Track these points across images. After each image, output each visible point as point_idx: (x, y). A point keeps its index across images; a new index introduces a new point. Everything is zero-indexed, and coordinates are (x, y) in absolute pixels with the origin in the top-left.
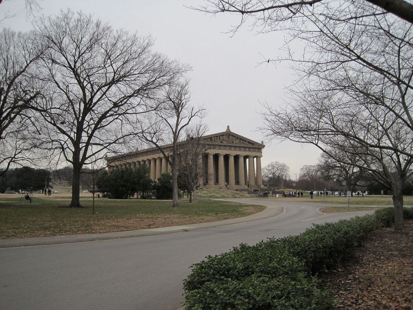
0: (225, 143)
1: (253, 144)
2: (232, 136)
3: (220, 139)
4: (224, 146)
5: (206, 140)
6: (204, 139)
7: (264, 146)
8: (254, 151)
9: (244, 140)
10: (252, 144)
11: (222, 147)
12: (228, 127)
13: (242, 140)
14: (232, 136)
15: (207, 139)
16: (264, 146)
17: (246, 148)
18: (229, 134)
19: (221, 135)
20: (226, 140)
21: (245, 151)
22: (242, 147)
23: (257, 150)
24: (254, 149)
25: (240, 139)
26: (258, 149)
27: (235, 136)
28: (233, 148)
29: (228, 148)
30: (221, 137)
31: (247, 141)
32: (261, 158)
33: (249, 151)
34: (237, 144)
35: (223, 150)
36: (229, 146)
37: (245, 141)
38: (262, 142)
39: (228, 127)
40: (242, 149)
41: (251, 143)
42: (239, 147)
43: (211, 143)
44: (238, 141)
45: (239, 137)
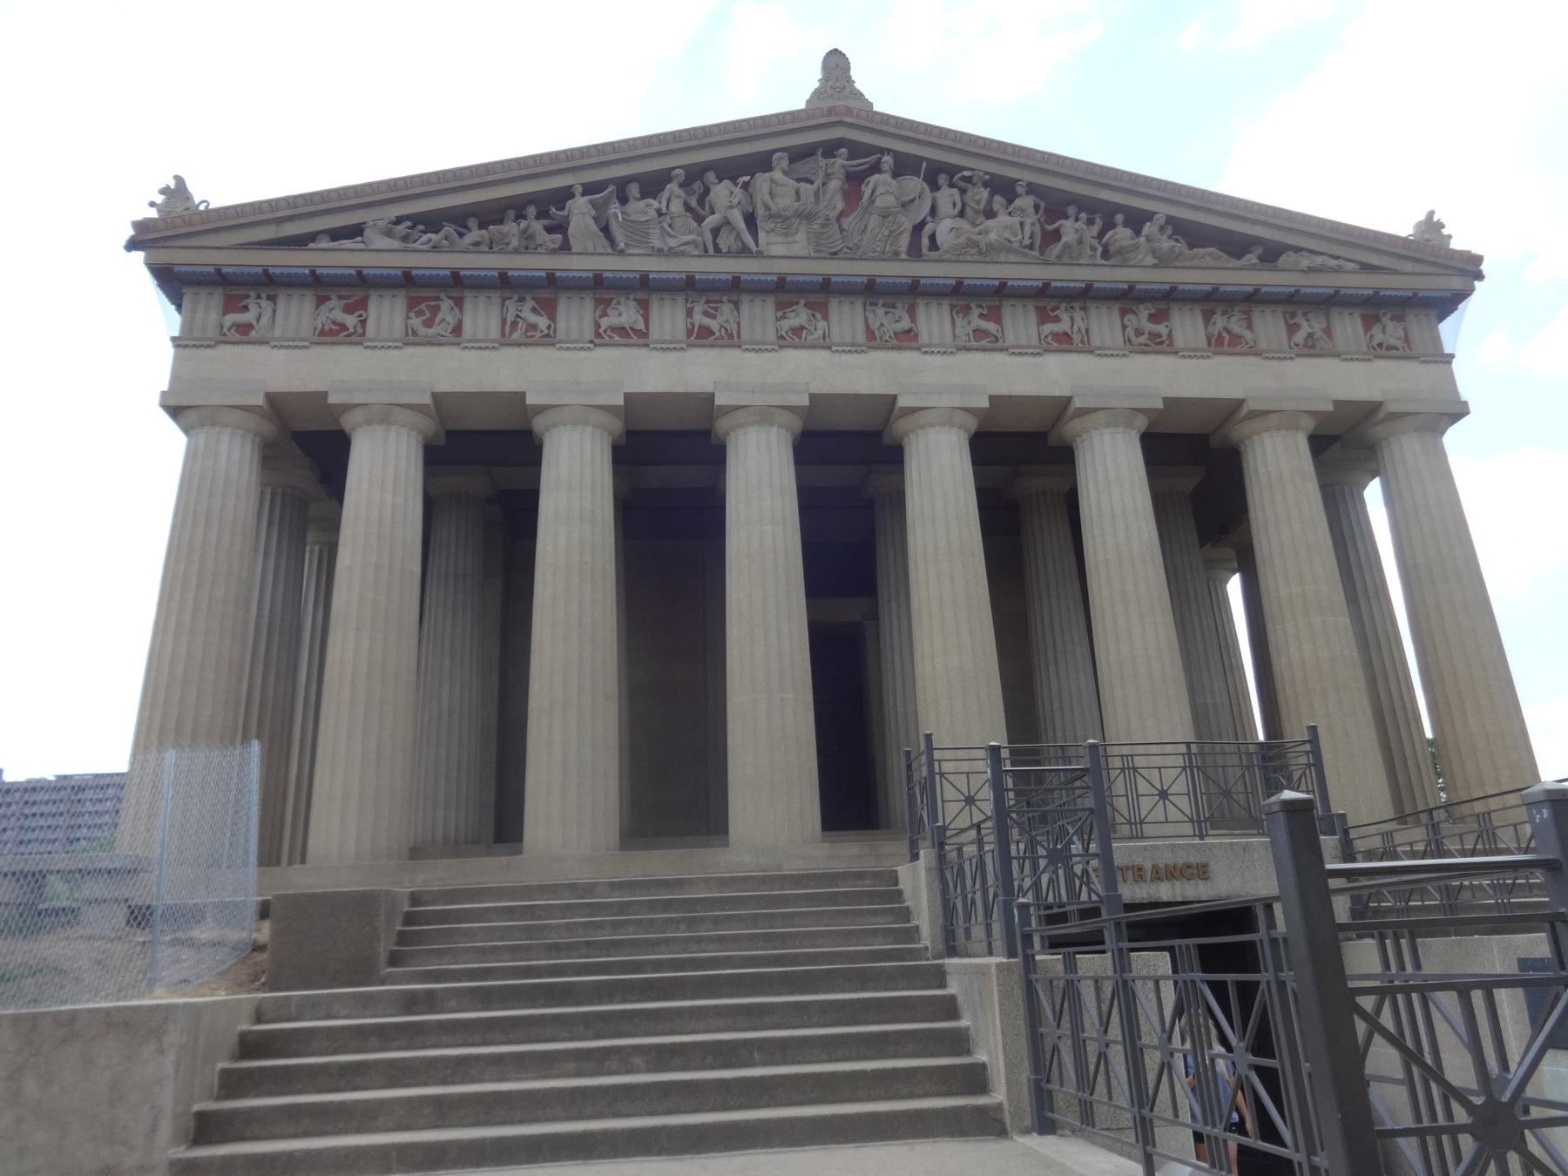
1: (1272, 254)
2: (904, 166)
3: (700, 220)
4: (782, 291)
5: (475, 235)
6: (431, 222)
7: (1469, 269)
10: (1251, 258)
11: (758, 316)
12: (836, 64)
14: (904, 166)
15: (490, 215)
16: (1469, 269)
18: (856, 150)
19: (730, 170)
20: (807, 217)
21: (1160, 345)
22: (1086, 295)
23: (1348, 328)
24: (1310, 325)
26: (1374, 307)
27: (952, 170)
29: (846, 319)
30: (722, 193)
31: (1163, 210)
32: (1454, 439)
33: (1222, 344)
34: (988, 253)
35: (758, 347)
36: (871, 291)
37: (1137, 220)
38: (1431, 226)
39: (836, 64)
40: (1104, 324)
41: (1236, 246)
42: (1046, 298)
43: (536, 263)
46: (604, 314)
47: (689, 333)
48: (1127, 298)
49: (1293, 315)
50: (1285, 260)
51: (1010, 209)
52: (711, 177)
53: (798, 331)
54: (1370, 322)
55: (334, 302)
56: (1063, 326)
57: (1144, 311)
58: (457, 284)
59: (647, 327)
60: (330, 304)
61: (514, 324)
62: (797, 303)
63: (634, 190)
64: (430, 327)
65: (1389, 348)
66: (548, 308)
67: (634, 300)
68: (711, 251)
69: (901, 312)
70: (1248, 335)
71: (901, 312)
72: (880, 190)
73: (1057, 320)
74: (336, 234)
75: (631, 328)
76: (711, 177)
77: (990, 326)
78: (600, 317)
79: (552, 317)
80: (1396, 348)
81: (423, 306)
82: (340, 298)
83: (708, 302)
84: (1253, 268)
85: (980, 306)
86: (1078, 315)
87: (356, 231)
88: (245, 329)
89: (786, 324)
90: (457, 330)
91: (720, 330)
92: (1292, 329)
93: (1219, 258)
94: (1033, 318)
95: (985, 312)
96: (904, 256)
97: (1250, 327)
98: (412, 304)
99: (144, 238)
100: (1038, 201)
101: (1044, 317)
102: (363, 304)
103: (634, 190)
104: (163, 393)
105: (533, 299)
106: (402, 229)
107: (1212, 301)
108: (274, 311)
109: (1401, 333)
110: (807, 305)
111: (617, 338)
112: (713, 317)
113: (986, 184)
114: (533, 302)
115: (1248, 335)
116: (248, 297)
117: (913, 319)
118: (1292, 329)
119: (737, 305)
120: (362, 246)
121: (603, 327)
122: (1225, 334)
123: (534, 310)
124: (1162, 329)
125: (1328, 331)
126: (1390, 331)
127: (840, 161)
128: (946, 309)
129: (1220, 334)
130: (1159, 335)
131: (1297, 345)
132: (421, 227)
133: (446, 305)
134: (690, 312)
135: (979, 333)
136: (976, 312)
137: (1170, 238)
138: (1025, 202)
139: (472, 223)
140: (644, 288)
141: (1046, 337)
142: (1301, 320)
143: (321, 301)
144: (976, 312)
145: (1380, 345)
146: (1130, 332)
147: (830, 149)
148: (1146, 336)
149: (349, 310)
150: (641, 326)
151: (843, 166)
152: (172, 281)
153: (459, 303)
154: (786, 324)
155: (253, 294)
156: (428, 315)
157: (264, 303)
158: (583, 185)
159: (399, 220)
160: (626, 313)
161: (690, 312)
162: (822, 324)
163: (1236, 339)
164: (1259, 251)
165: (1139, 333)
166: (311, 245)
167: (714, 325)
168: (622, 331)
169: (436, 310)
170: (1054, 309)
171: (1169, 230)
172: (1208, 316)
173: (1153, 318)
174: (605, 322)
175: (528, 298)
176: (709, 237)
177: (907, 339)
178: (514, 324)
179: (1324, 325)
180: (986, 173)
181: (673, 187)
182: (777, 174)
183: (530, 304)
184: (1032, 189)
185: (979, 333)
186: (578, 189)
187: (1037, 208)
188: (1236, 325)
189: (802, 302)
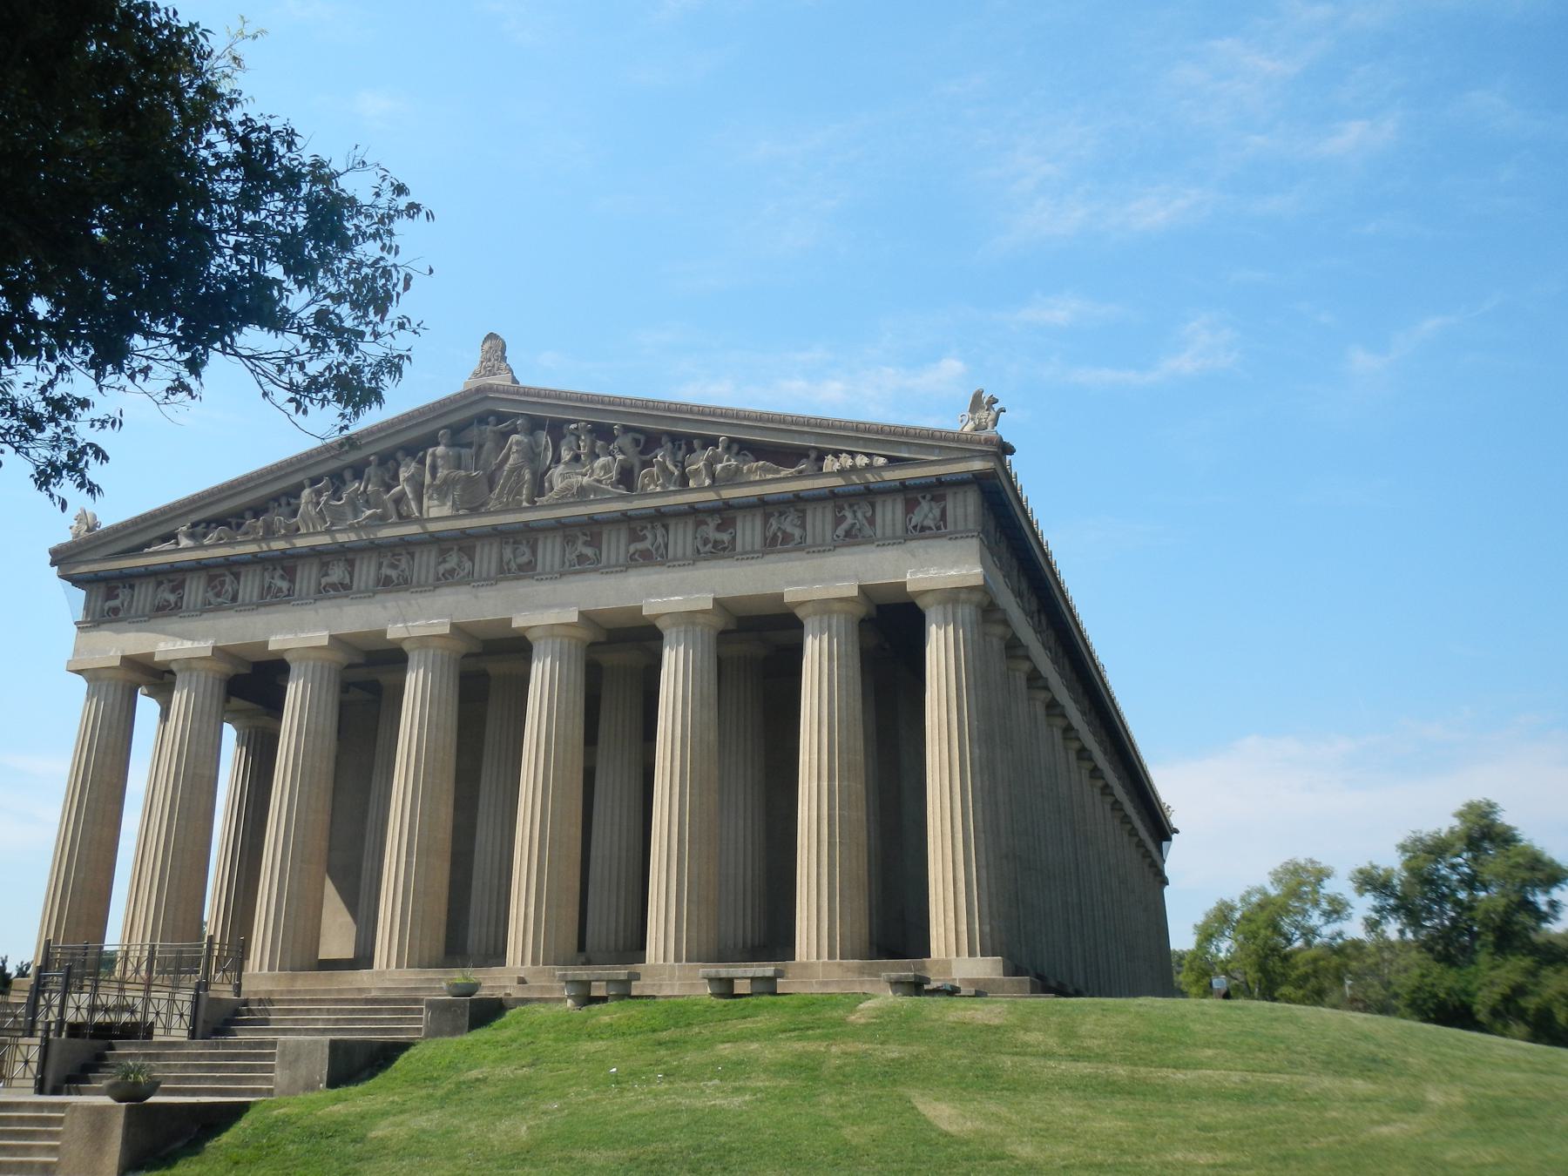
0: (438, 513)
4: (440, 542)
8: (852, 538)
9: (685, 443)
12: (495, 347)
13: (675, 438)
14: (535, 424)
15: (258, 510)
17: (726, 513)
18: (501, 417)
21: (720, 551)
22: (660, 517)
25: (648, 442)
26: (910, 493)
28: (550, 552)
33: (774, 544)
39: (495, 347)
40: (681, 538)
41: (783, 456)
44: (603, 468)
45: (617, 423)
46: (326, 575)
47: (378, 581)
48: (694, 513)
49: (841, 509)
50: (830, 464)
51: (611, 447)
52: (400, 455)
53: (451, 572)
54: (910, 506)
55: (165, 585)
56: (646, 545)
57: (713, 522)
58: (233, 566)
59: (352, 582)
60: (162, 588)
61: (270, 587)
62: (452, 549)
63: (348, 475)
64: (219, 597)
65: (923, 529)
66: (290, 575)
67: (346, 560)
68: (394, 519)
69: (524, 548)
70: (797, 533)
71: (524, 548)
72: (514, 448)
73: (644, 538)
74: (165, 539)
75: (341, 584)
76: (400, 455)
77: (589, 551)
78: (323, 576)
79: (292, 581)
80: (930, 528)
81: (217, 582)
82: (170, 581)
83: (393, 555)
84: (801, 475)
85: (585, 535)
86: (660, 531)
87: (171, 537)
88: (115, 611)
89: (441, 569)
90: (234, 599)
91: (398, 578)
92: (839, 521)
93: (769, 471)
94: (623, 541)
95: (589, 539)
96: (525, 504)
97: (803, 526)
98: (211, 579)
99: (62, 558)
100: (638, 436)
101: (635, 537)
102: (181, 585)
103: (348, 475)
104: (69, 661)
105: (283, 569)
106: (200, 529)
107: (763, 505)
108: (133, 596)
109: (937, 512)
110: (460, 549)
111: (332, 592)
112: (394, 566)
113: (590, 432)
114: (281, 572)
115: (797, 533)
116: (118, 587)
117: (534, 553)
118: (839, 521)
119: (412, 555)
120: (173, 547)
121: (323, 583)
122: (779, 534)
123: (282, 577)
124: (725, 537)
125: (872, 522)
126: (926, 512)
127: (489, 428)
128: (558, 540)
129: (775, 534)
130: (723, 542)
131: (838, 537)
132: (213, 525)
133: (228, 579)
134: (380, 565)
135: (581, 558)
136: (582, 539)
137: (738, 454)
138: (625, 441)
139: (248, 514)
140: (345, 554)
141: (634, 554)
142: (848, 514)
143: (160, 584)
144: (580, 542)
145: (915, 527)
146: (699, 543)
147: (482, 419)
148: (710, 545)
149: (173, 591)
150: (347, 580)
151: (491, 431)
152: (76, 581)
153: (237, 576)
154: (441, 569)
155: (121, 585)
156: (219, 588)
157: (127, 591)
158: (310, 479)
159: (194, 525)
160: (337, 574)
161: (380, 565)
162: (468, 565)
163: (787, 538)
164: (813, 455)
165: (706, 542)
166: (146, 550)
167: (393, 573)
168: (334, 586)
169: (223, 583)
170: (641, 531)
171: (735, 448)
172: (766, 518)
173: (719, 528)
174: (324, 581)
175: (279, 568)
176: (391, 507)
177: (527, 570)
178: (270, 587)
179: (869, 514)
180: (589, 422)
181: (370, 471)
182: (440, 450)
183: (279, 572)
184: (626, 429)
185: (581, 558)
186: (307, 483)
187: (637, 442)
188: (789, 525)
189: (456, 548)
